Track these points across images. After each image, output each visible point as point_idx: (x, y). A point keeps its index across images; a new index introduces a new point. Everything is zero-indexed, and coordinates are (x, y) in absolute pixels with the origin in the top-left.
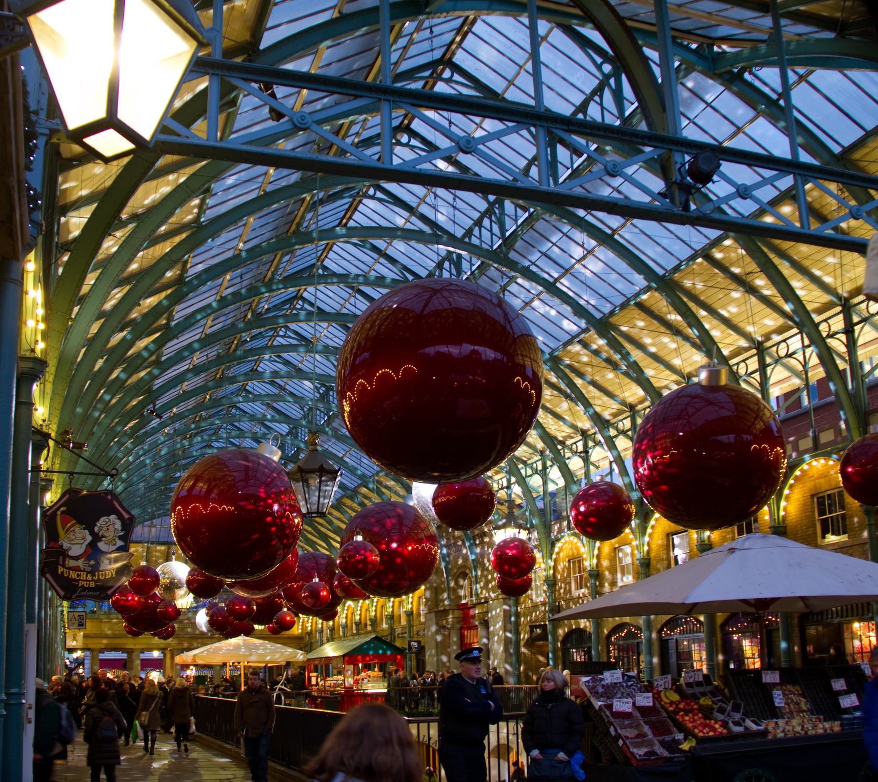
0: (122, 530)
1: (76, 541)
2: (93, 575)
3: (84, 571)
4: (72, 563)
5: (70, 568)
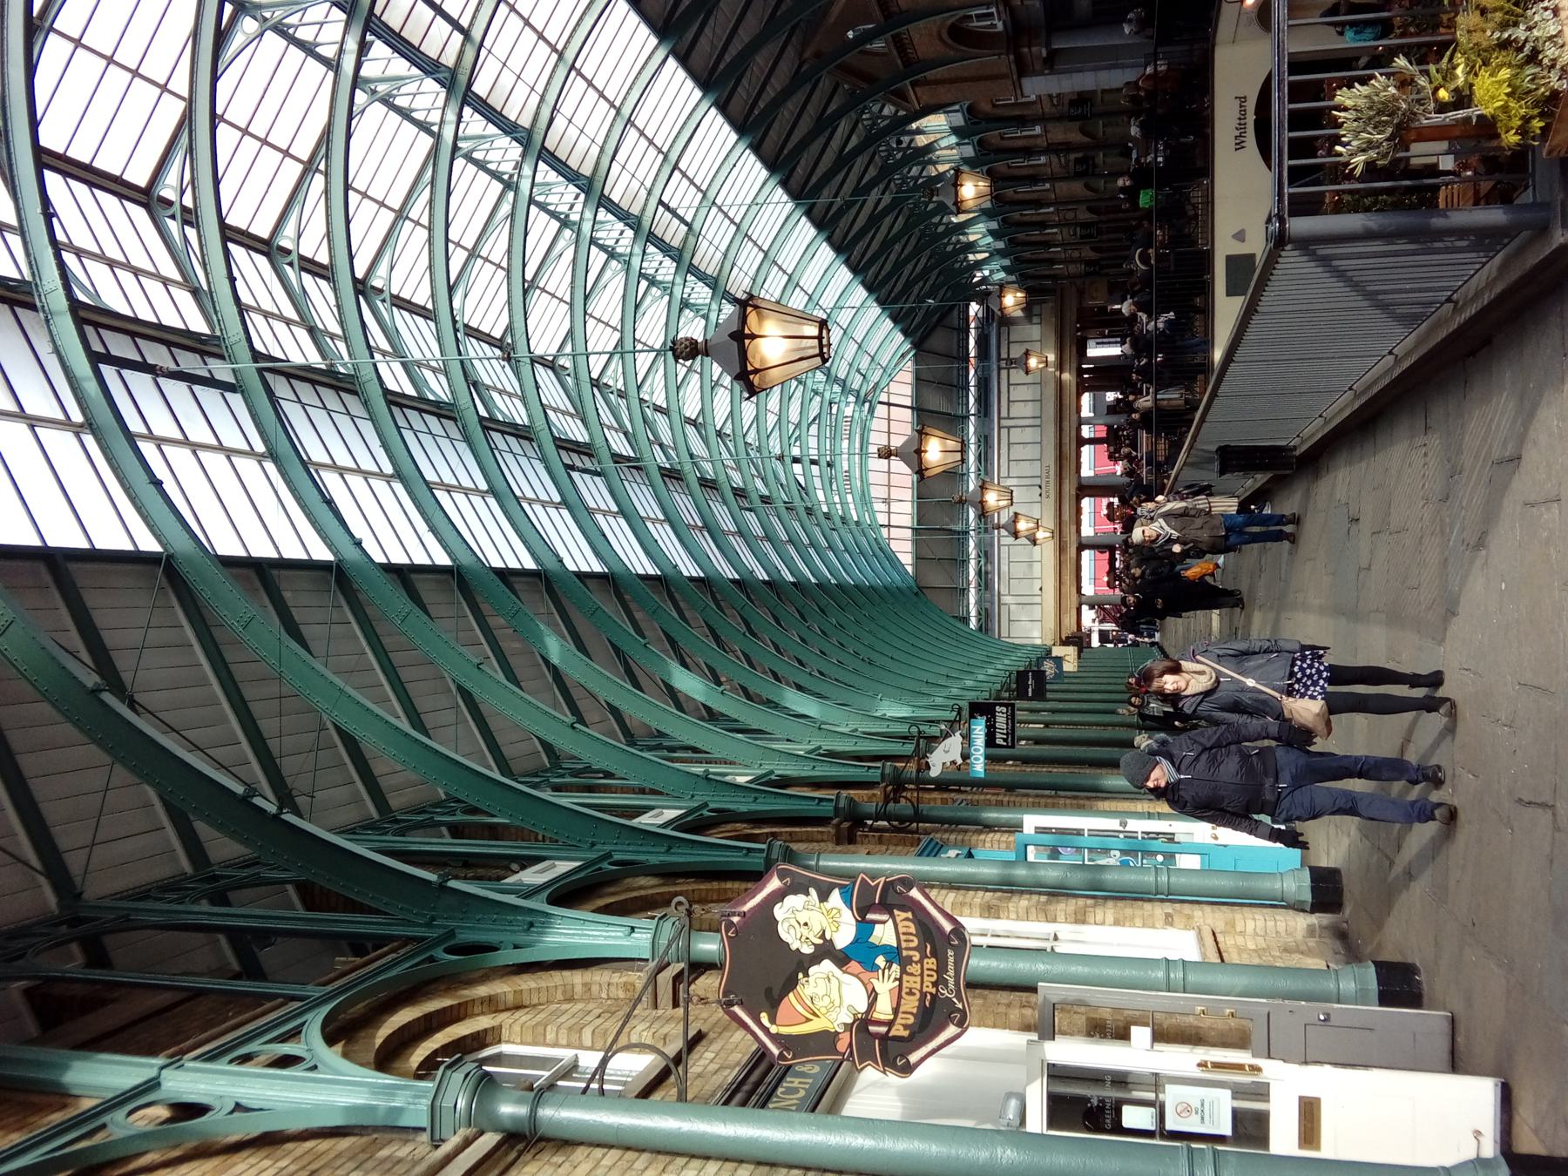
0: (807, 894)
1: (835, 996)
3: (900, 980)
4: (884, 1009)
5: (896, 1011)
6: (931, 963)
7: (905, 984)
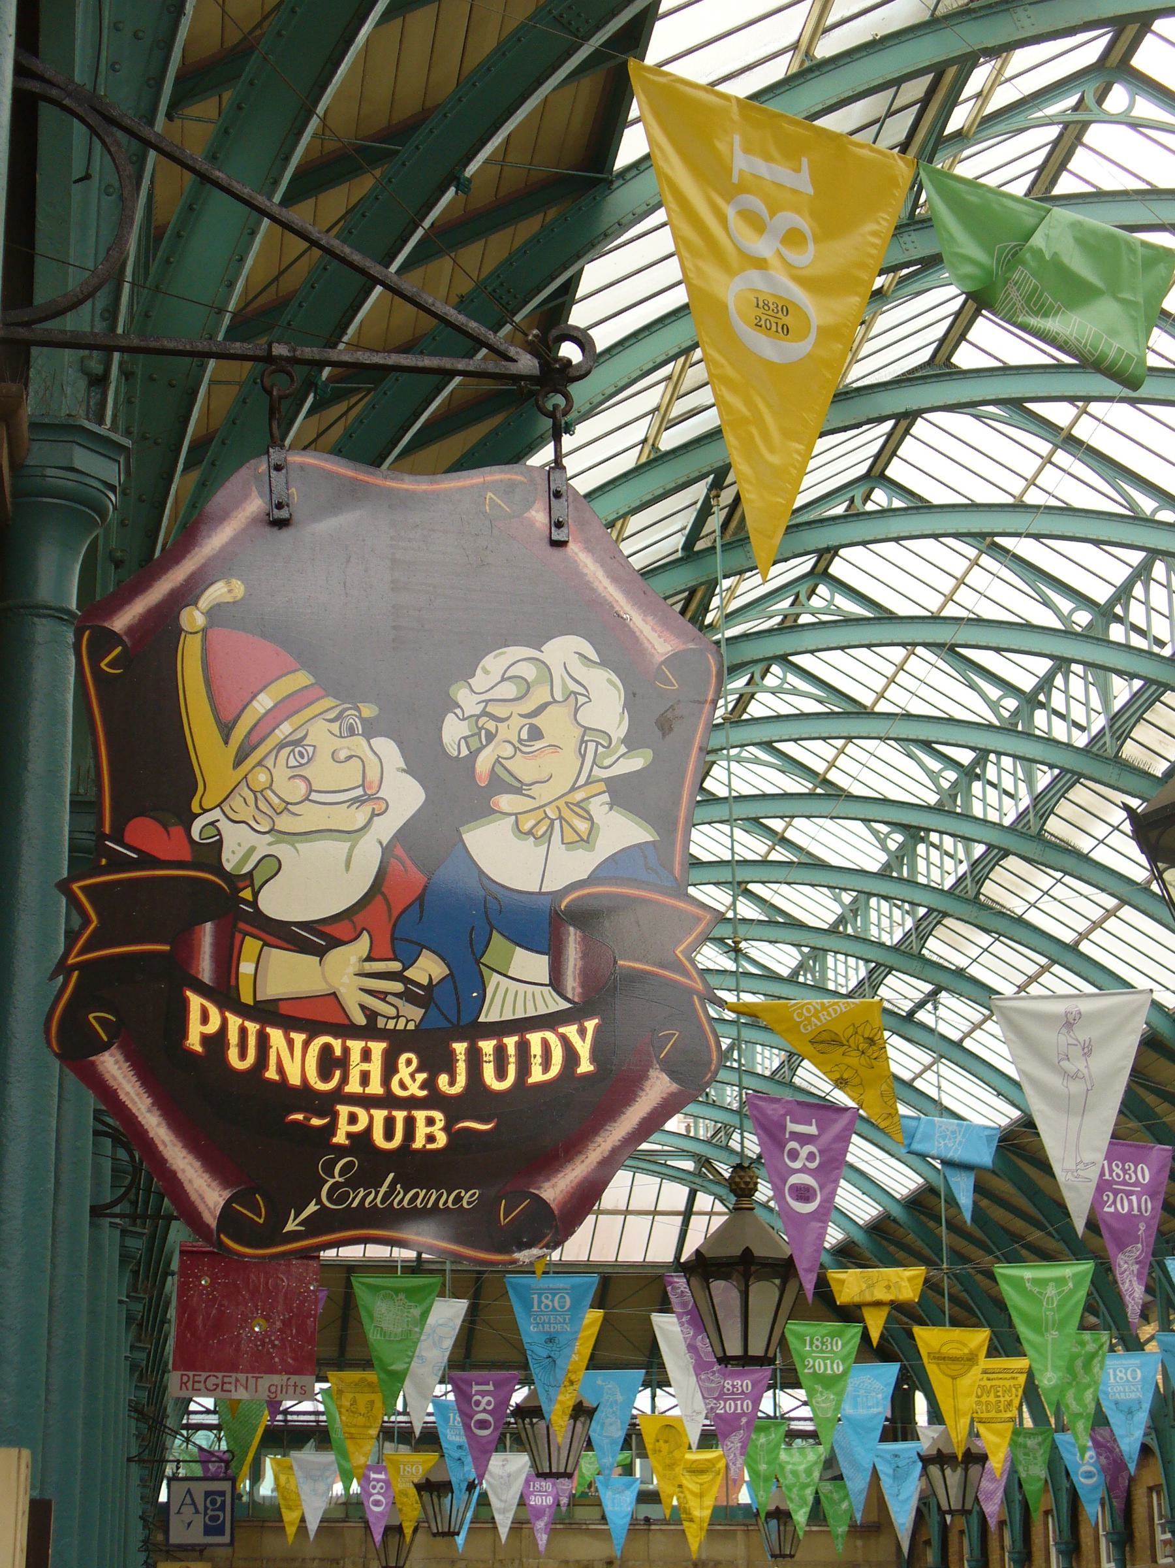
0: (632, 742)
2: (436, 1061)
3: (370, 1031)
4: (284, 974)
5: (268, 1013)
7: (356, 1046)
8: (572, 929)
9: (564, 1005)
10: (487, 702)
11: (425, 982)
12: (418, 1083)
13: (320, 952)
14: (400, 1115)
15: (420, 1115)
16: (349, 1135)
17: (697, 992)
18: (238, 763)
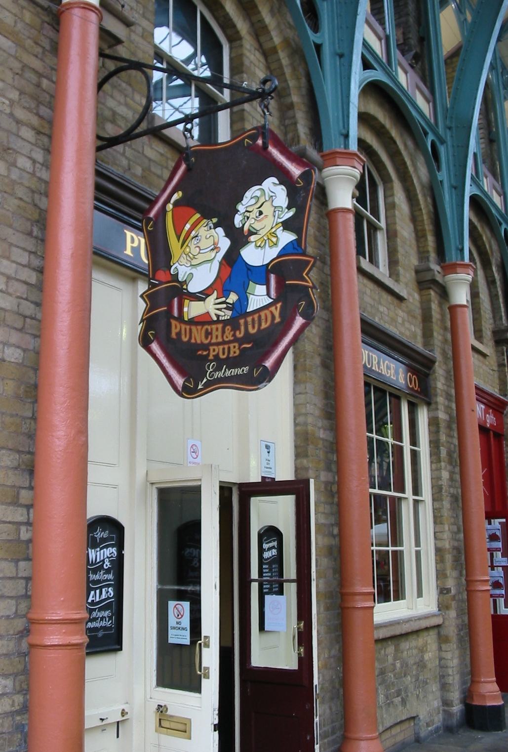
1: (201, 258)
6: (235, 351)
7: (214, 327)
8: (272, 275)
9: (271, 301)
10: (247, 207)
11: (232, 302)
12: (231, 335)
13: (203, 300)
14: (226, 347)
15: (232, 345)
16: (214, 356)
17: (310, 287)
18: (182, 247)
